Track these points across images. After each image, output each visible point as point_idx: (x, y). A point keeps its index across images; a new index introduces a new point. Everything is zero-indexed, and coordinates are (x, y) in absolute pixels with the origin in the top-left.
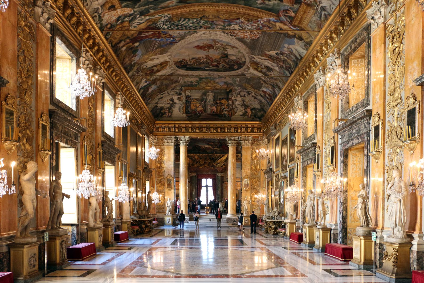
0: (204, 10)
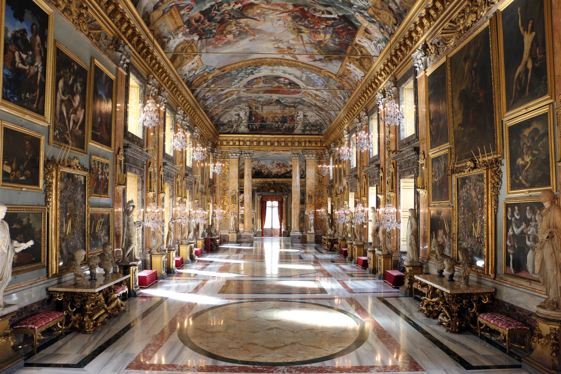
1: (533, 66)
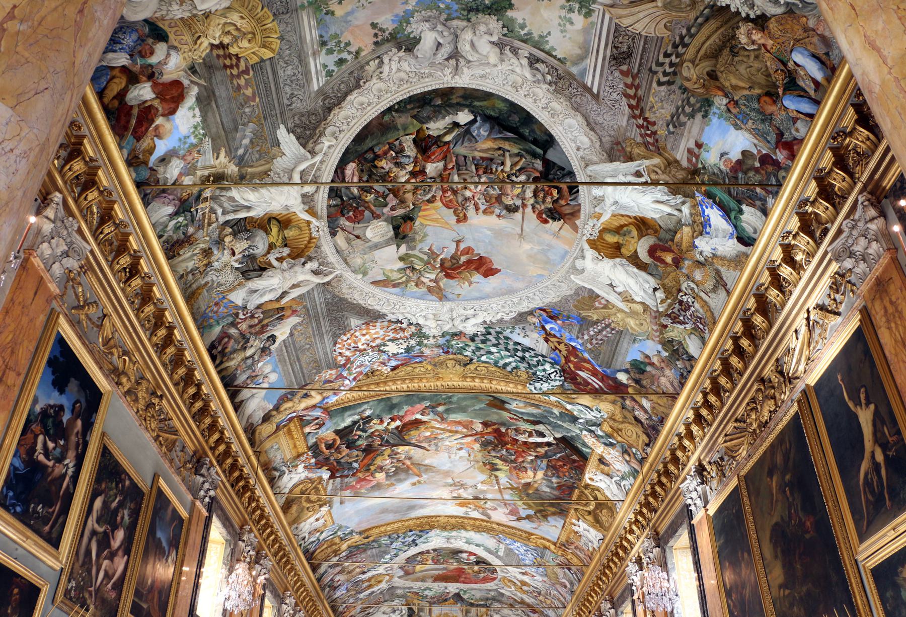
0: (465, 377)
1: (886, 457)
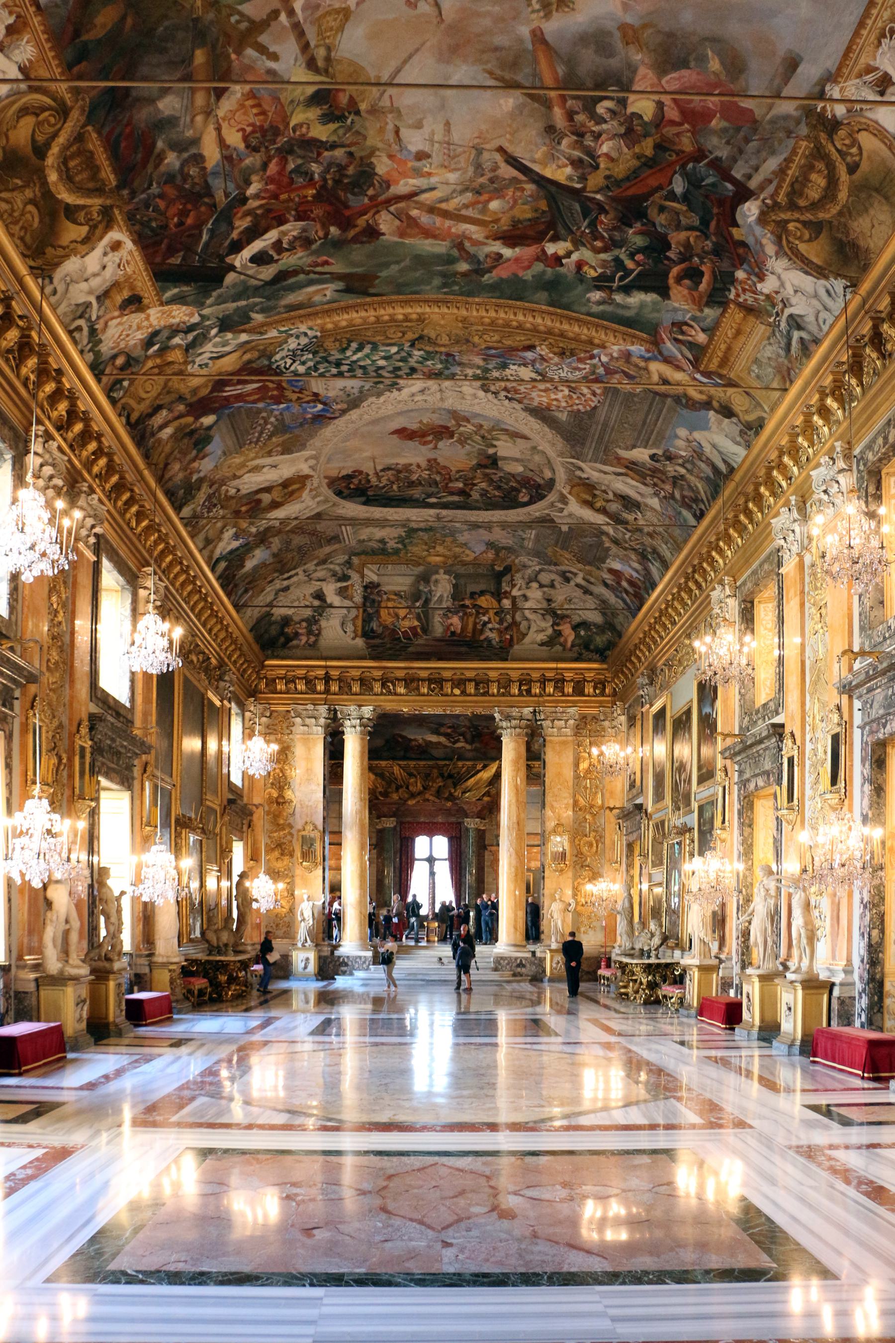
0: (421, 319)
